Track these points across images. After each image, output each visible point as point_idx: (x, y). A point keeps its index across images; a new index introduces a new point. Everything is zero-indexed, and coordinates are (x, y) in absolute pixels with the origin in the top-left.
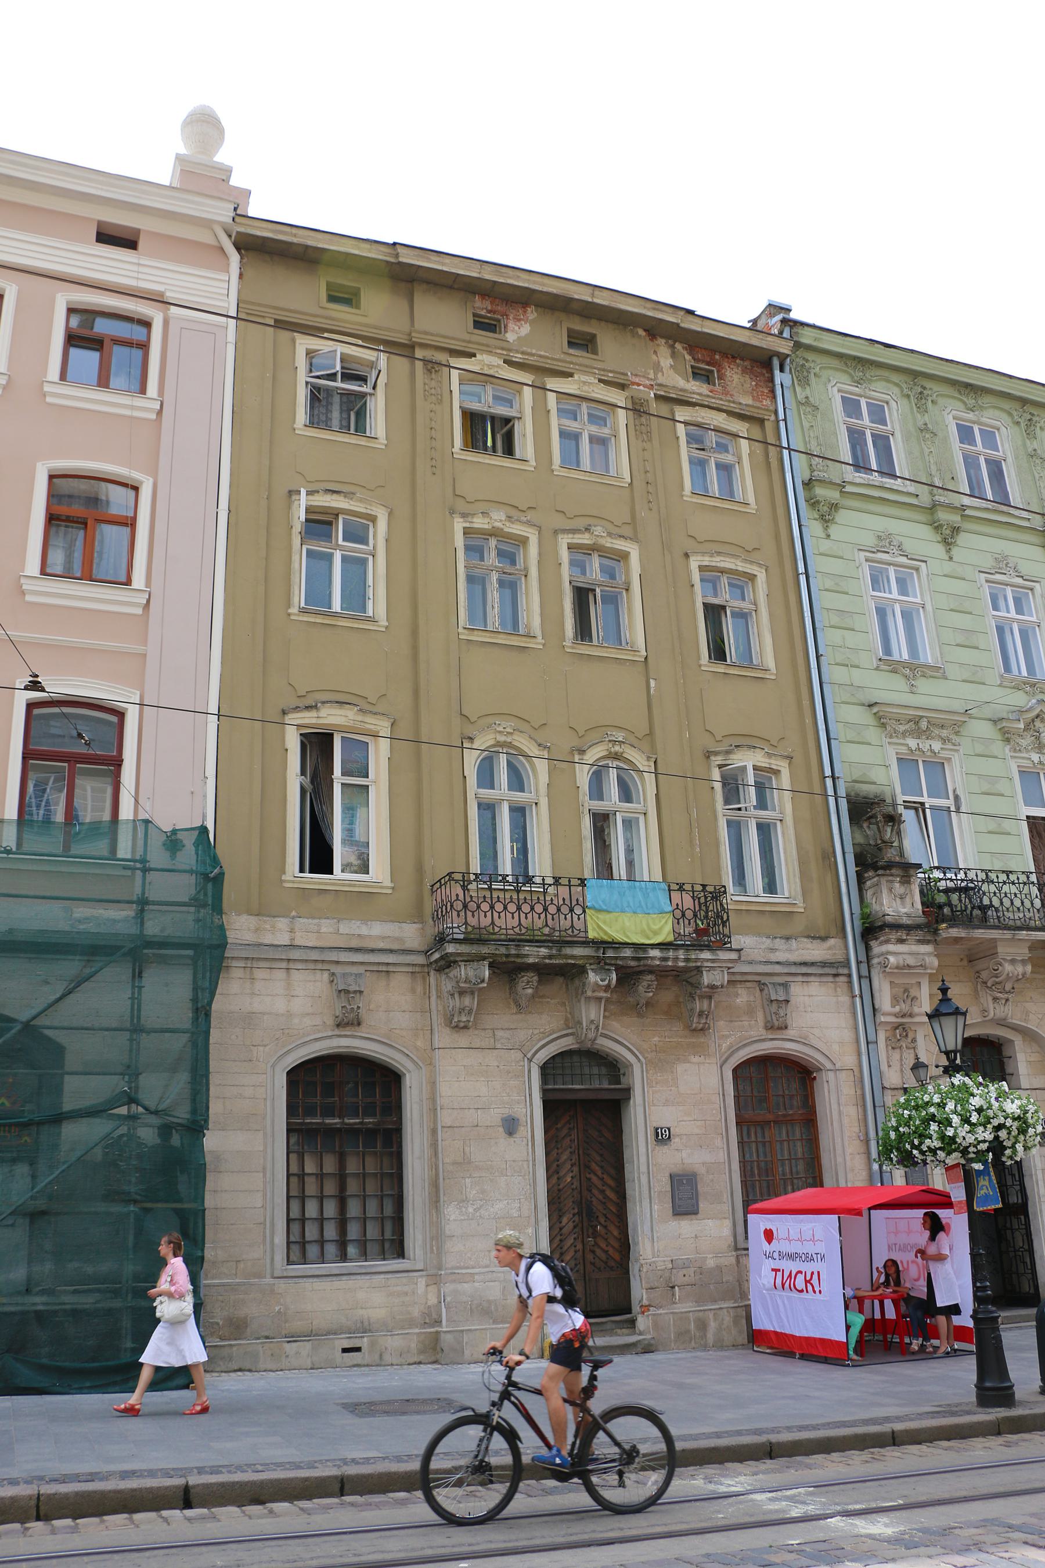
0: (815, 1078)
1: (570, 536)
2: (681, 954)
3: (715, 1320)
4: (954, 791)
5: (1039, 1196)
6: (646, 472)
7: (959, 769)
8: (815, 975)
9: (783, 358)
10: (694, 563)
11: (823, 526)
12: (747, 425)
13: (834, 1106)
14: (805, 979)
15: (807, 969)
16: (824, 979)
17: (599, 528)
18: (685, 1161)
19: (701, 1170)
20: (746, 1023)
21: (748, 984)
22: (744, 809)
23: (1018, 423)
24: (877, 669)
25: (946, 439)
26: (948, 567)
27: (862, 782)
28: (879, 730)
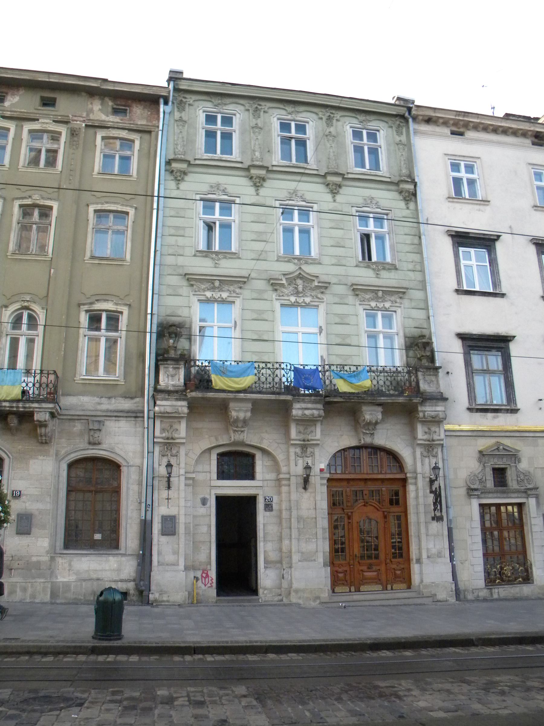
1: (21, 201)
2: (21, 405)
3: (32, 587)
6: (71, 165)
7: (238, 306)
8: (123, 417)
10: (91, 209)
12: (140, 135)
14: (117, 419)
15: (118, 415)
17: (37, 195)
18: (27, 508)
19: (36, 513)
20: (78, 441)
21: (82, 421)
24: (195, 256)
27: (172, 316)
28: (189, 289)
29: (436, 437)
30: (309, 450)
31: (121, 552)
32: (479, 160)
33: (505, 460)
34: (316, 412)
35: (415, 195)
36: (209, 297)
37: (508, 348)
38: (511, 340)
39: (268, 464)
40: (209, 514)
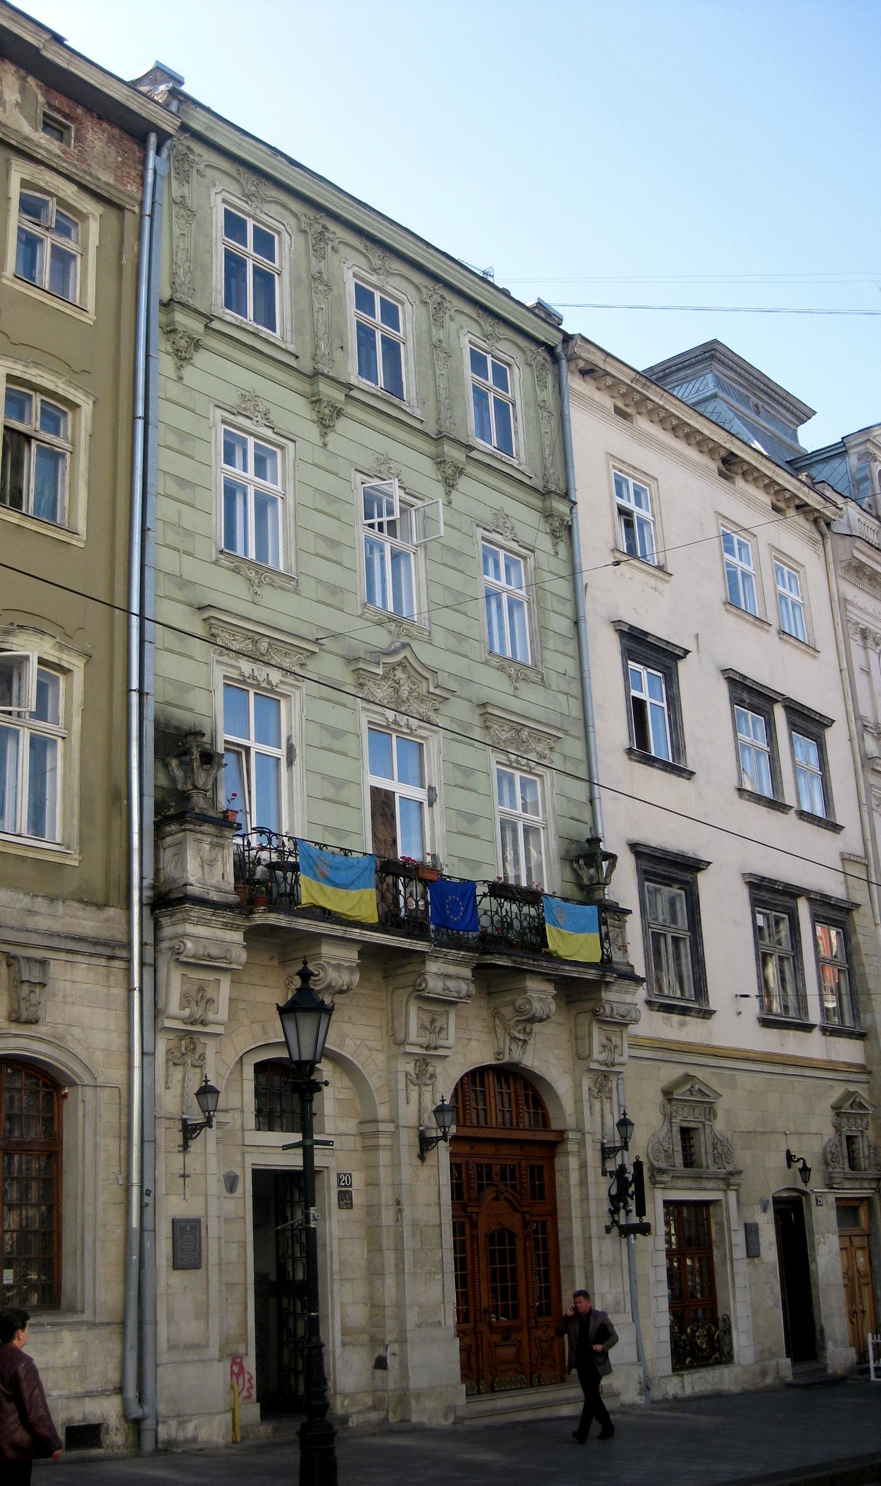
0: (65, 1096)
4: (289, 739)
5: (332, 1272)
8: (83, 954)
9: (163, 137)
11: (176, 364)
13: (89, 1135)
14: (69, 957)
16: (95, 961)
22: (15, 714)
23: (425, 303)
24: (216, 562)
25: (341, 299)
26: (320, 457)
27: (176, 706)
29: (618, 1059)
30: (430, 1069)
31: (87, 1316)
32: (655, 482)
33: (697, 1111)
34: (464, 987)
35: (570, 528)
36: (247, 675)
37: (695, 883)
38: (700, 869)
39: (341, 1097)
40: (240, 1214)
